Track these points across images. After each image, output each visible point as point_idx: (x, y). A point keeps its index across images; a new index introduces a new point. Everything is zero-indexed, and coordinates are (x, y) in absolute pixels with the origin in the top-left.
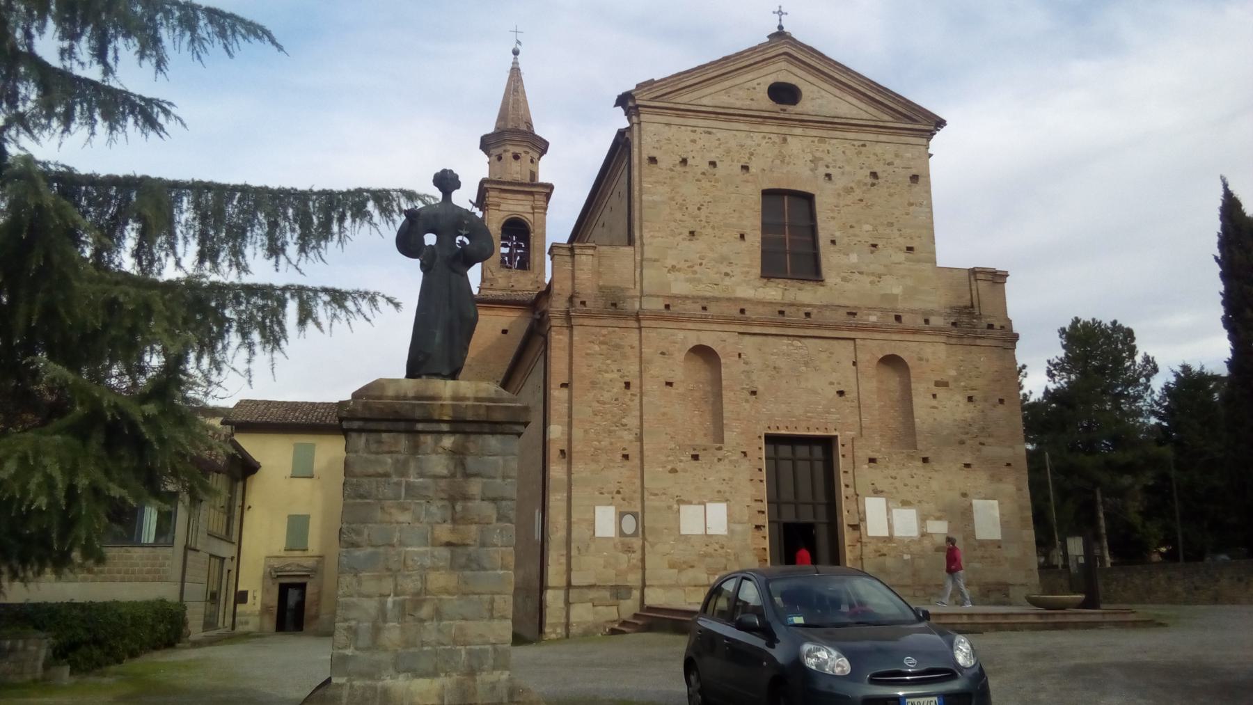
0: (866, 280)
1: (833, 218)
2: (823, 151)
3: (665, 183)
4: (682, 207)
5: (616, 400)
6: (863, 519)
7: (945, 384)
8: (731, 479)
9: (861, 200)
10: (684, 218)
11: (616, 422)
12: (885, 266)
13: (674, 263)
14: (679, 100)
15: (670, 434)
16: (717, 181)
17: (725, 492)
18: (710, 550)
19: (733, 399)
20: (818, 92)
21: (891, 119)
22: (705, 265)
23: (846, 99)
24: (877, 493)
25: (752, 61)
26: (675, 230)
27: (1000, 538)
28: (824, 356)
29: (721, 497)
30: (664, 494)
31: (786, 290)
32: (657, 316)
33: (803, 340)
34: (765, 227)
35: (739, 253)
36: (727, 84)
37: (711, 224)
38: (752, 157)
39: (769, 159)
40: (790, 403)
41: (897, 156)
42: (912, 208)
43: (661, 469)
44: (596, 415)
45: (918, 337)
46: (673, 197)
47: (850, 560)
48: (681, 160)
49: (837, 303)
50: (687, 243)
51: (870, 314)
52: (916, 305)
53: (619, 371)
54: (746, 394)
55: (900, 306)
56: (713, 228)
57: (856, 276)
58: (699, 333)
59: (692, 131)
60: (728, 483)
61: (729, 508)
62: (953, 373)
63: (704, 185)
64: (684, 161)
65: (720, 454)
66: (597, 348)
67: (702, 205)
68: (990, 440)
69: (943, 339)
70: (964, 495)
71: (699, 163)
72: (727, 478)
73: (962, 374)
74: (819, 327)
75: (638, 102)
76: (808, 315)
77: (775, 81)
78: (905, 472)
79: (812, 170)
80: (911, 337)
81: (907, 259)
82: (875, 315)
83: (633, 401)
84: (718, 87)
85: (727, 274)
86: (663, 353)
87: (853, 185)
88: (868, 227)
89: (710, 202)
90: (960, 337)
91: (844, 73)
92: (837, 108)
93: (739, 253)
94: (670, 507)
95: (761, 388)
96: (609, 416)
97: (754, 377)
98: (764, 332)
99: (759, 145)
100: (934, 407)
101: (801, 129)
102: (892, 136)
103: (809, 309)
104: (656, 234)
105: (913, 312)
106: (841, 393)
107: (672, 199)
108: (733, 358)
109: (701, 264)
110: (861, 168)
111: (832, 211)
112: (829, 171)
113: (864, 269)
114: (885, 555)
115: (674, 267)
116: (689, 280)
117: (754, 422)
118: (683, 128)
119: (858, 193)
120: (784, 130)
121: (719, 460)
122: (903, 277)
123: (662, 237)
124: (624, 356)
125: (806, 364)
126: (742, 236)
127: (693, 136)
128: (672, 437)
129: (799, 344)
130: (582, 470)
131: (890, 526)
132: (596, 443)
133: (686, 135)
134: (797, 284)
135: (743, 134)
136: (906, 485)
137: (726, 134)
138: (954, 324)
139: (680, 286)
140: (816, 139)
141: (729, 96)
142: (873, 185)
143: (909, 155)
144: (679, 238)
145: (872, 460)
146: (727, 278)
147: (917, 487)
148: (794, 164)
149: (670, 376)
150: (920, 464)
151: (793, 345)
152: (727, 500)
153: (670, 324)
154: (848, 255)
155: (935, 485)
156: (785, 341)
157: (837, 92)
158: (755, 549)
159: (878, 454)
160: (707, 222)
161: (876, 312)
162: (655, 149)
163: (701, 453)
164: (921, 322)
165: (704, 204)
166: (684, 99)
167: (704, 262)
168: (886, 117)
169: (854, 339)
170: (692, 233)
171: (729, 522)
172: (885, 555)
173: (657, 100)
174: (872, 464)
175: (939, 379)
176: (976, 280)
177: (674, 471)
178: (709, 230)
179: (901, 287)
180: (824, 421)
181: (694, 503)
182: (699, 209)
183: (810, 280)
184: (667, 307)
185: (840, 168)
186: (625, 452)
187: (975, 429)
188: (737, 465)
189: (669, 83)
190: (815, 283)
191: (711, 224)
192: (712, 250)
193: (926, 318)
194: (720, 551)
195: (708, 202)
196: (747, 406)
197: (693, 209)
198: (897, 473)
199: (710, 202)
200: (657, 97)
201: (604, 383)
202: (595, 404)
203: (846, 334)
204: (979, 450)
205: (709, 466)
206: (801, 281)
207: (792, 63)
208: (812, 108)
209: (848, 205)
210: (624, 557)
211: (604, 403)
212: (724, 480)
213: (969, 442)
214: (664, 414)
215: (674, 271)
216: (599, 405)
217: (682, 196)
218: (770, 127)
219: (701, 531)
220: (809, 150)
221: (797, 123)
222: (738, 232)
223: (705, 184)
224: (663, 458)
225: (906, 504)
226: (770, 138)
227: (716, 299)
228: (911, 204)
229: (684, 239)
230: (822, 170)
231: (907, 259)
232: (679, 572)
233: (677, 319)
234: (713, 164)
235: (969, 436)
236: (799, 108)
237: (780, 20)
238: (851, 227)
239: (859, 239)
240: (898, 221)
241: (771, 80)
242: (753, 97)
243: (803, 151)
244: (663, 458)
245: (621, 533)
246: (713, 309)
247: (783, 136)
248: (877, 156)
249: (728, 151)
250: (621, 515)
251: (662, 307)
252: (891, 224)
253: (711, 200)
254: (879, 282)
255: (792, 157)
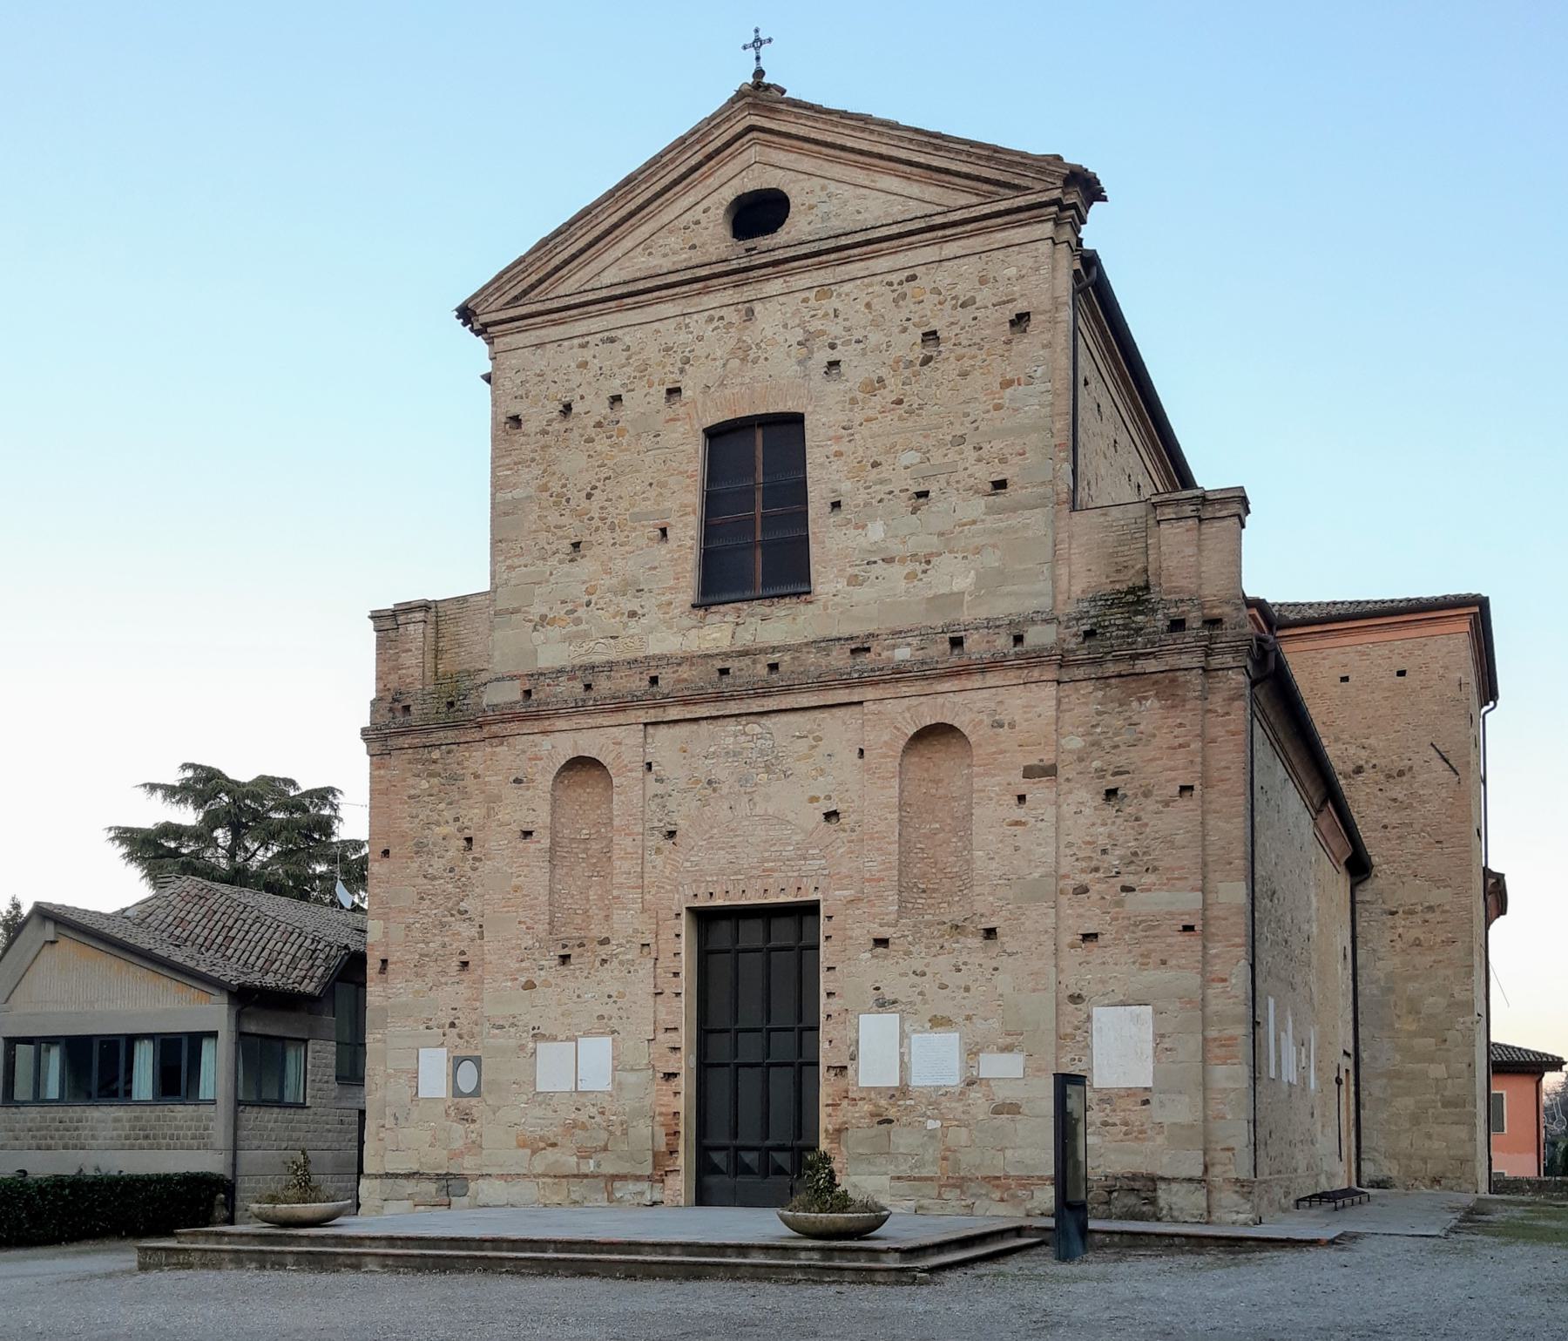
0: (898, 571)
1: (838, 454)
2: (826, 314)
3: (533, 460)
4: (561, 500)
5: (452, 870)
6: (853, 1058)
7: (1049, 771)
8: (622, 995)
9: (900, 402)
10: (564, 521)
11: (452, 909)
12: (941, 534)
13: (545, 610)
14: (561, 290)
15: (524, 923)
16: (621, 433)
17: (610, 1018)
18: (583, 1117)
19: (629, 850)
20: (823, 188)
21: (975, 200)
22: (596, 604)
23: (878, 186)
24: (883, 1004)
25: (683, 169)
26: (547, 547)
27: (1149, 1084)
28: (802, 746)
29: (604, 1026)
30: (513, 1025)
31: (737, 624)
32: (510, 715)
33: (764, 720)
34: (712, 502)
35: (655, 568)
36: (646, 229)
37: (609, 521)
38: (687, 367)
39: (717, 363)
40: (734, 847)
41: (983, 281)
42: (1009, 390)
43: (509, 984)
44: (422, 898)
45: (992, 679)
46: (546, 484)
47: (826, 1131)
48: (561, 408)
49: (835, 634)
50: (567, 567)
51: (894, 647)
52: (1003, 607)
53: (456, 819)
54: (657, 840)
55: (966, 616)
56: (612, 528)
57: (879, 568)
58: (578, 735)
59: (583, 346)
60: (615, 1002)
61: (615, 1047)
62: (1076, 743)
63: (599, 448)
64: (567, 409)
65: (604, 951)
66: (425, 785)
67: (594, 488)
68: (1149, 879)
69: (1051, 673)
70: (1076, 999)
71: (592, 406)
72: (614, 994)
73: (1095, 744)
74: (788, 690)
75: (484, 319)
76: (773, 667)
77: (740, 193)
78: (944, 961)
79: (800, 363)
80: (976, 680)
81: (990, 510)
82: (909, 645)
83: (474, 869)
84: (628, 243)
85: (633, 614)
86: (518, 781)
87: (884, 372)
88: (911, 457)
89: (609, 478)
90: (1095, 662)
91: (863, 130)
92: (859, 212)
93: (655, 568)
94: (522, 1047)
95: (682, 825)
96: (440, 900)
97: (671, 805)
98: (689, 716)
99: (700, 339)
100: (1017, 823)
101: (781, 280)
102: (971, 239)
103: (774, 658)
104: (516, 561)
105: (991, 625)
106: (831, 816)
107: (544, 488)
108: (634, 774)
109: (588, 604)
110: (905, 330)
111: (838, 438)
112: (835, 356)
113: (896, 548)
114: (890, 1121)
115: (543, 617)
116: (569, 639)
117: (669, 887)
118: (566, 343)
119: (894, 387)
120: (749, 292)
121: (605, 961)
122: (978, 551)
123: (526, 566)
124: (464, 792)
125: (768, 768)
126: (664, 531)
127: (587, 354)
128: (527, 928)
129: (757, 729)
130: (402, 991)
131: (904, 1067)
132: (422, 945)
133: (569, 357)
134: (760, 608)
135: (672, 324)
136: (943, 987)
137: (639, 333)
138: (1089, 634)
139: (553, 653)
140: (812, 294)
141: (650, 254)
142: (926, 361)
143: (1012, 271)
144: (554, 561)
145: (882, 942)
146: (632, 622)
147: (967, 989)
148: (766, 359)
149: (525, 819)
150: (976, 942)
151: (745, 734)
152: (613, 1032)
153: (527, 727)
154: (864, 527)
155: (1003, 982)
156: (732, 726)
157: (860, 176)
158: (661, 1114)
159: (892, 930)
160: (602, 519)
161: (909, 640)
162: (518, 400)
163: (574, 952)
164: (1003, 642)
165: (598, 484)
166: (570, 285)
167: (594, 598)
168: (964, 199)
169: (861, 703)
170: (576, 545)
171: (615, 1069)
172: (890, 1121)
173: (521, 302)
174: (880, 950)
175: (1033, 761)
176: (1158, 522)
177: (530, 985)
178: (606, 535)
179: (972, 572)
180: (796, 874)
181: (559, 1039)
182: (589, 496)
183: (783, 596)
184: (528, 693)
185: (858, 342)
186: (464, 958)
187: (1113, 860)
188: (632, 969)
189: (531, 264)
190: (794, 600)
191: (609, 521)
192: (608, 572)
193: (1016, 632)
194: (598, 1119)
195: (606, 478)
196: (659, 860)
197: (578, 498)
198: (927, 965)
199: (609, 478)
200: (516, 298)
201: (435, 845)
202: (421, 880)
203: (842, 696)
204: (1119, 904)
205: (585, 974)
206: (767, 602)
207: (768, 144)
208: (808, 229)
209: (869, 420)
210: (459, 1129)
211: (434, 878)
212: (610, 996)
213: (1095, 888)
214: (517, 889)
215: (543, 626)
216: (426, 881)
217: (560, 479)
218: (719, 294)
219: (570, 1087)
220: (797, 322)
221: (770, 270)
222: (655, 526)
223: (602, 445)
224: (514, 965)
225: (938, 1022)
226: (722, 318)
227: (611, 666)
228: (1006, 384)
229: (561, 562)
230: (824, 356)
231: (990, 510)
232: (534, 1152)
233: (537, 717)
234: (616, 399)
235: (1100, 875)
236: (782, 236)
237: (758, 58)
238: (875, 465)
239: (889, 488)
240: (977, 428)
241: (729, 194)
242: (695, 241)
243: (785, 326)
244: (514, 965)
245: (457, 1092)
246: (603, 686)
247: (747, 305)
248: (940, 294)
249: (644, 368)
250: (457, 1062)
251: (518, 696)
252: (960, 440)
253: (611, 473)
254: (925, 572)
255: (763, 345)
